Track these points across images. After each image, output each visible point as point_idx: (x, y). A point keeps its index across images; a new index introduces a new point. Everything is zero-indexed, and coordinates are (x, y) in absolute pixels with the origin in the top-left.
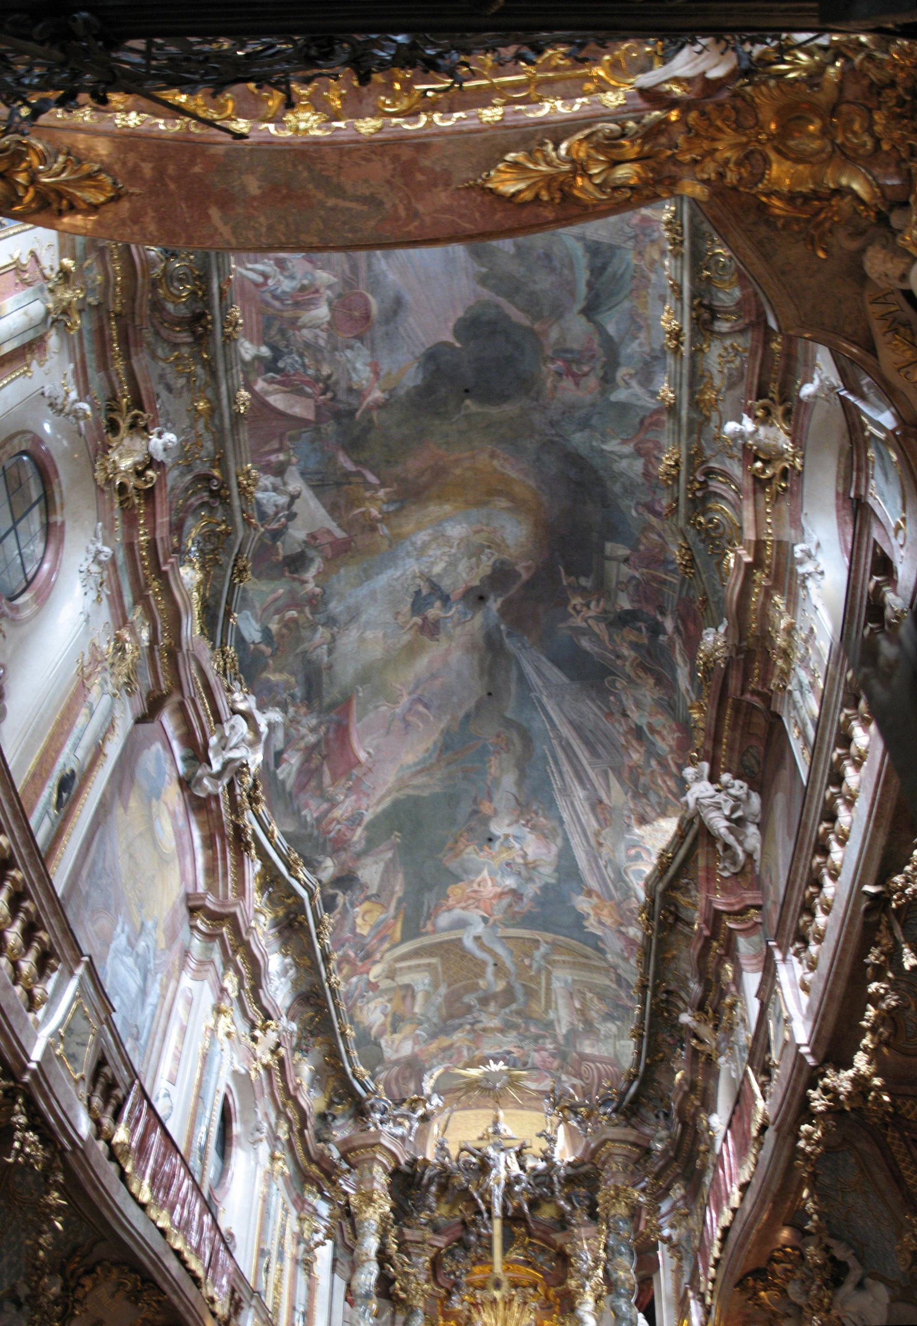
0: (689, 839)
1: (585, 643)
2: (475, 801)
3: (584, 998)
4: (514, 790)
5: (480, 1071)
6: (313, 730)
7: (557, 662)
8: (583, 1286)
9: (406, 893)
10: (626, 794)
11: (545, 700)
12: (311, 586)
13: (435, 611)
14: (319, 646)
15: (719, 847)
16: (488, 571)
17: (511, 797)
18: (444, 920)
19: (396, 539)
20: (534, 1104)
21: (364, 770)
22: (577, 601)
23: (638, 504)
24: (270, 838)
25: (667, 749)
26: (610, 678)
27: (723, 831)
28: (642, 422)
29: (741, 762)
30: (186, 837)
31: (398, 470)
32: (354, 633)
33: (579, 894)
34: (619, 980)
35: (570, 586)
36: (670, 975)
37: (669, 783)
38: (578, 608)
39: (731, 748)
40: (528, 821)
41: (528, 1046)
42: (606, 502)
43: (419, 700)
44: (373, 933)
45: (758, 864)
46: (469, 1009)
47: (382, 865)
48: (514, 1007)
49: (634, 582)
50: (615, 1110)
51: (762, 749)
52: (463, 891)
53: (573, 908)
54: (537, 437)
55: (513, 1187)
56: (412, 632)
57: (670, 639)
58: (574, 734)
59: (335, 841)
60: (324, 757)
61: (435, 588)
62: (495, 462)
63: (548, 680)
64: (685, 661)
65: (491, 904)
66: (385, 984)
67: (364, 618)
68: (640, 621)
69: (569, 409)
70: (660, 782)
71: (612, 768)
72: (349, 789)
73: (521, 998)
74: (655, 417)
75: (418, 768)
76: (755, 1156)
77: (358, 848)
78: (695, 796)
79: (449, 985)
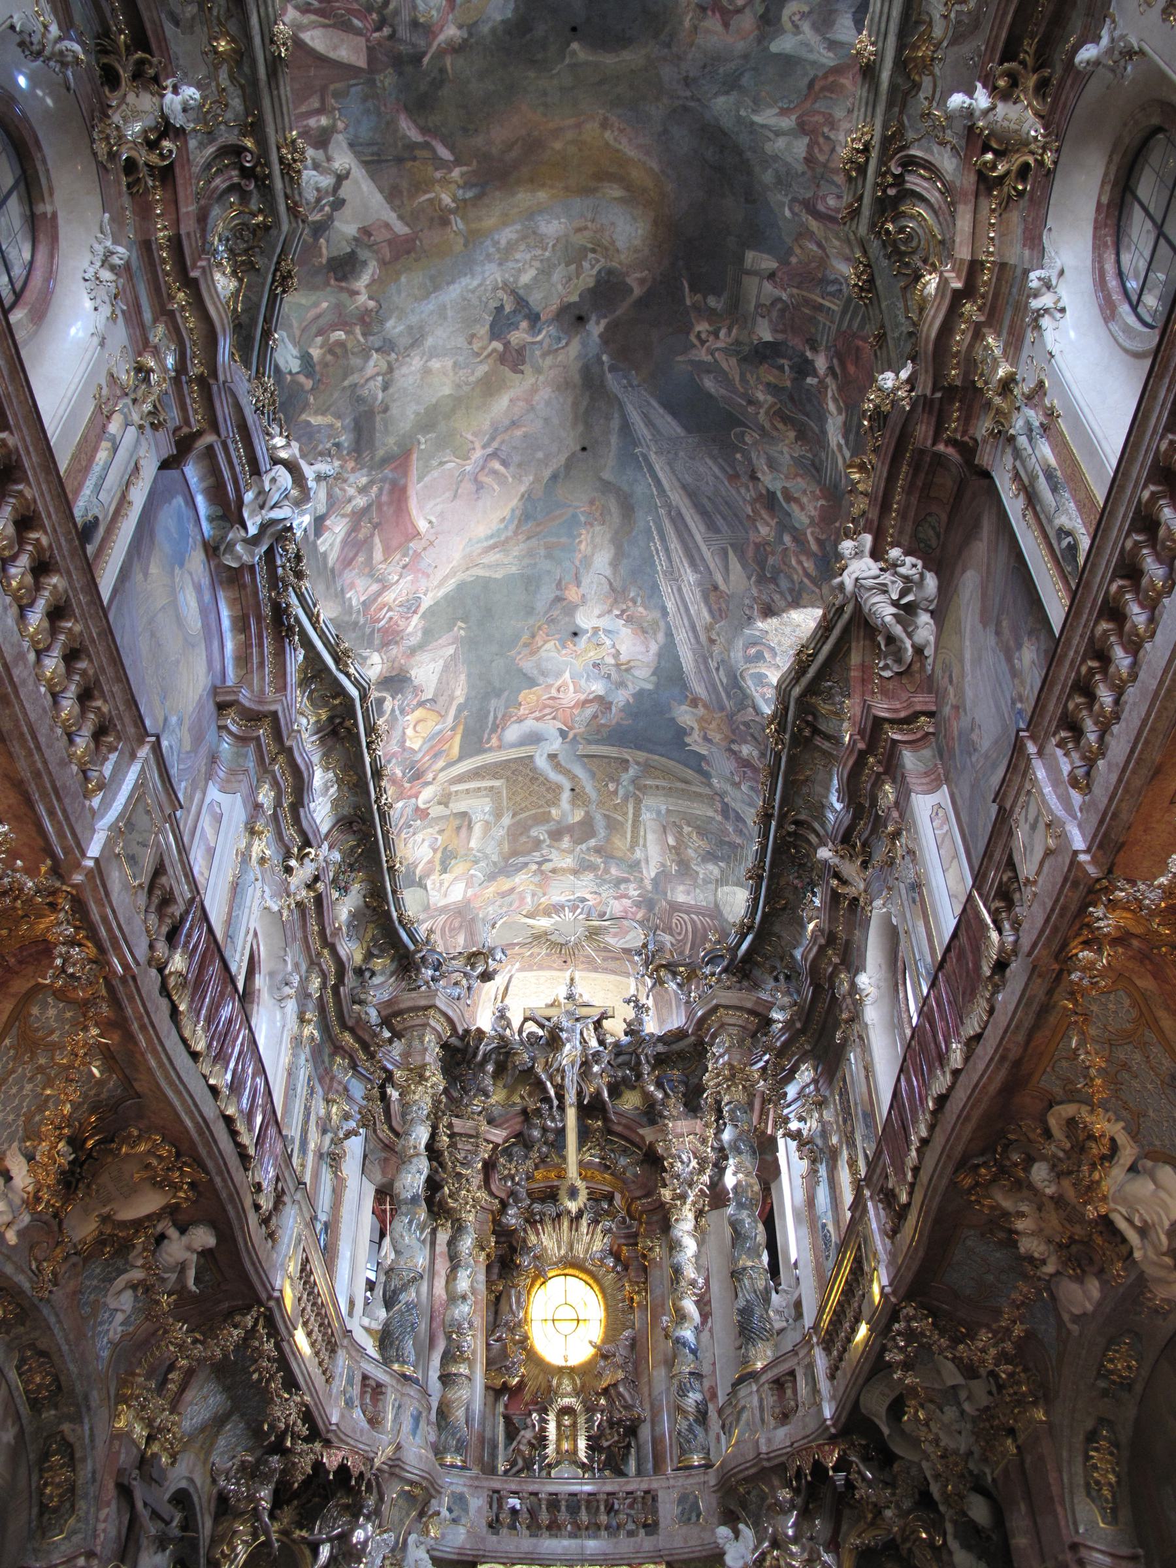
1: (709, 384)
2: (559, 585)
3: (681, 833)
4: (608, 572)
5: (552, 921)
6: (363, 490)
7: (672, 408)
8: (683, 1197)
9: (467, 699)
10: (749, 578)
11: (653, 457)
12: (362, 298)
13: (519, 335)
14: (372, 378)
15: (881, 639)
16: (591, 283)
17: (604, 580)
18: (513, 733)
19: (473, 238)
20: (612, 965)
21: (424, 543)
22: (702, 327)
23: (794, 200)
24: (315, 624)
25: (807, 521)
26: (738, 430)
27: (888, 619)
28: (811, 85)
29: (915, 535)
30: (213, 616)
31: (478, 141)
32: (416, 362)
33: (681, 703)
34: (726, 811)
35: (695, 306)
36: (800, 802)
38: (703, 336)
39: (903, 515)
40: (623, 612)
41: (607, 892)
42: (751, 196)
43: (494, 455)
44: (426, 747)
45: (930, 661)
46: (537, 844)
47: (441, 662)
48: (592, 842)
49: (779, 306)
50: (725, 970)
51: (944, 517)
52: (539, 698)
53: (673, 720)
54: (665, 100)
55: (591, 1067)
56: (490, 361)
57: (821, 382)
58: (687, 501)
59: (385, 631)
60: (375, 527)
61: (521, 303)
62: (607, 134)
63: (658, 432)
64: (840, 412)
65: (572, 714)
66: (436, 811)
67: (429, 342)
68: (783, 357)
69: (713, 61)
70: (794, 562)
71: (732, 545)
72: (404, 567)
73: (602, 832)
75: (491, 542)
76: (988, 1000)
77: (414, 641)
78: (854, 576)
79: (514, 815)
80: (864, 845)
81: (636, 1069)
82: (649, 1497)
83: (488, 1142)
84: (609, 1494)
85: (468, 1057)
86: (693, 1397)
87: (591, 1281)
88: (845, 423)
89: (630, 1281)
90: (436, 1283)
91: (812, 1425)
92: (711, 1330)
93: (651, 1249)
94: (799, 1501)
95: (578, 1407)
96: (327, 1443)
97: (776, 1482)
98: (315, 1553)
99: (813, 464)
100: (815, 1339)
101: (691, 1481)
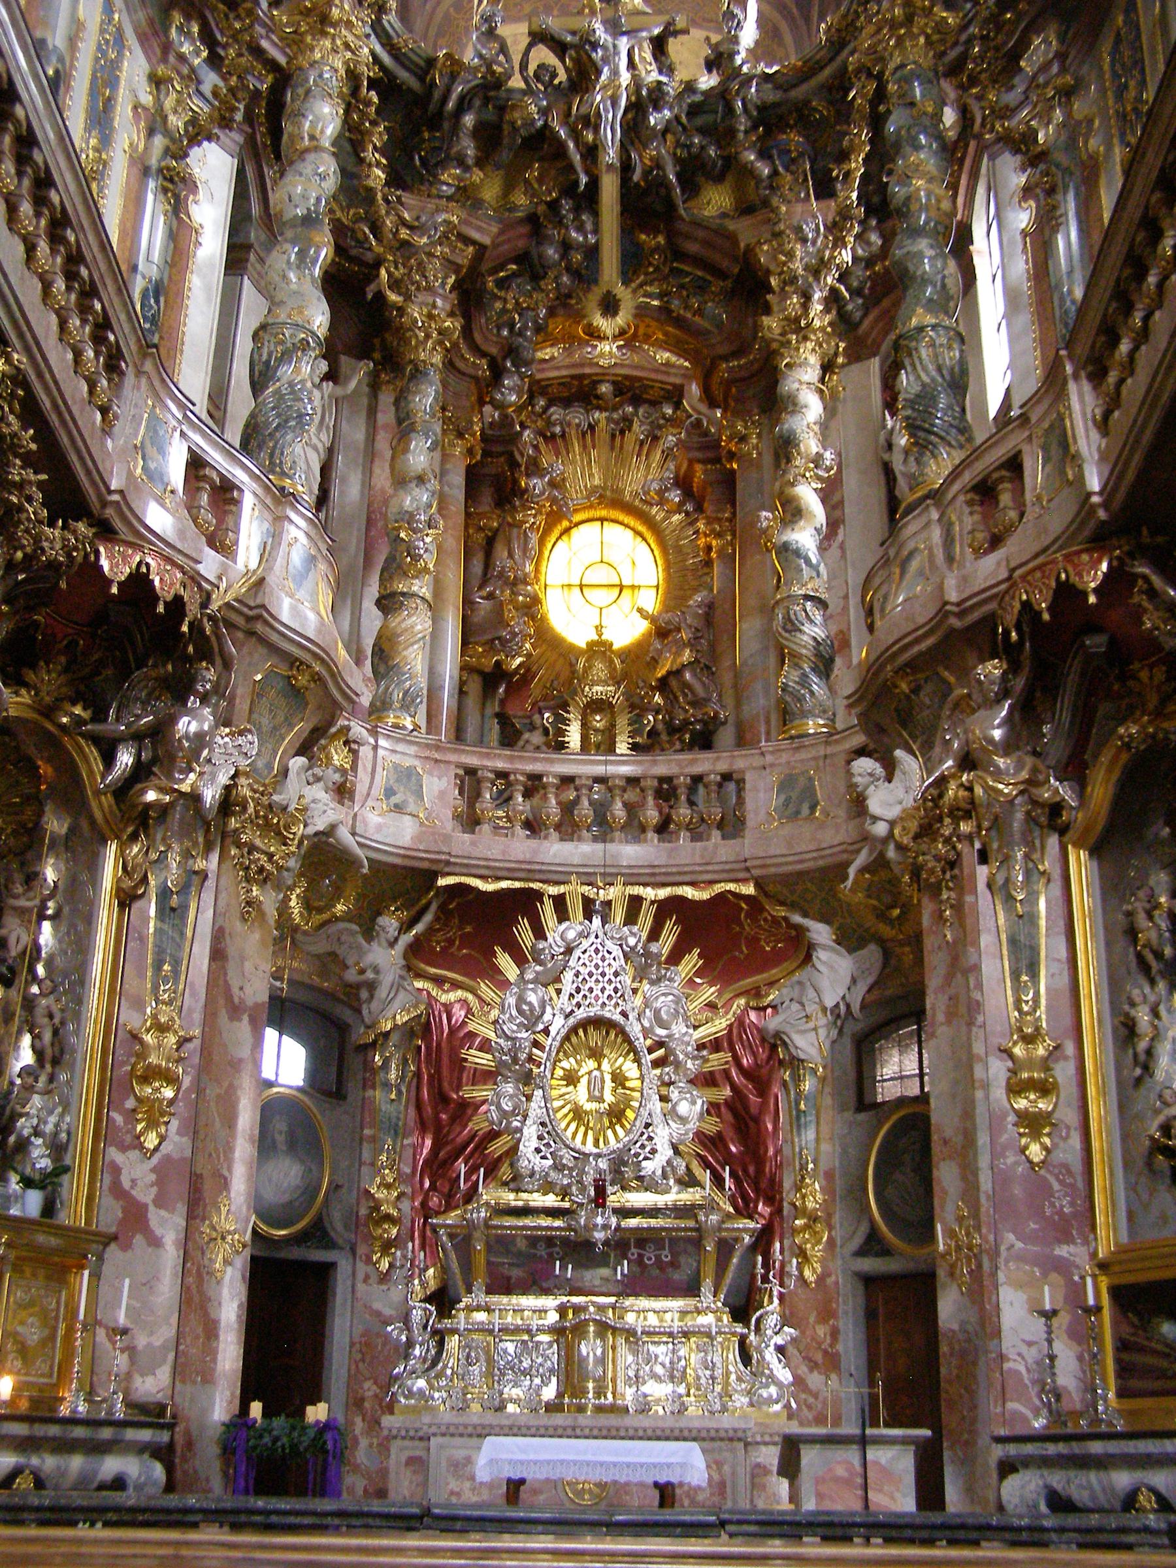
81: (724, 135)
82: (731, 787)
83: (467, 240)
84: (662, 780)
85: (432, 108)
86: (814, 629)
87: (641, 528)
89: (707, 518)
90: (377, 471)
91: (1058, 521)
92: (842, 547)
93: (743, 439)
94: (1019, 683)
95: (618, 699)
96: (106, 531)
97: (971, 658)
98: (109, 759)
100: (1069, 369)
101: (803, 755)
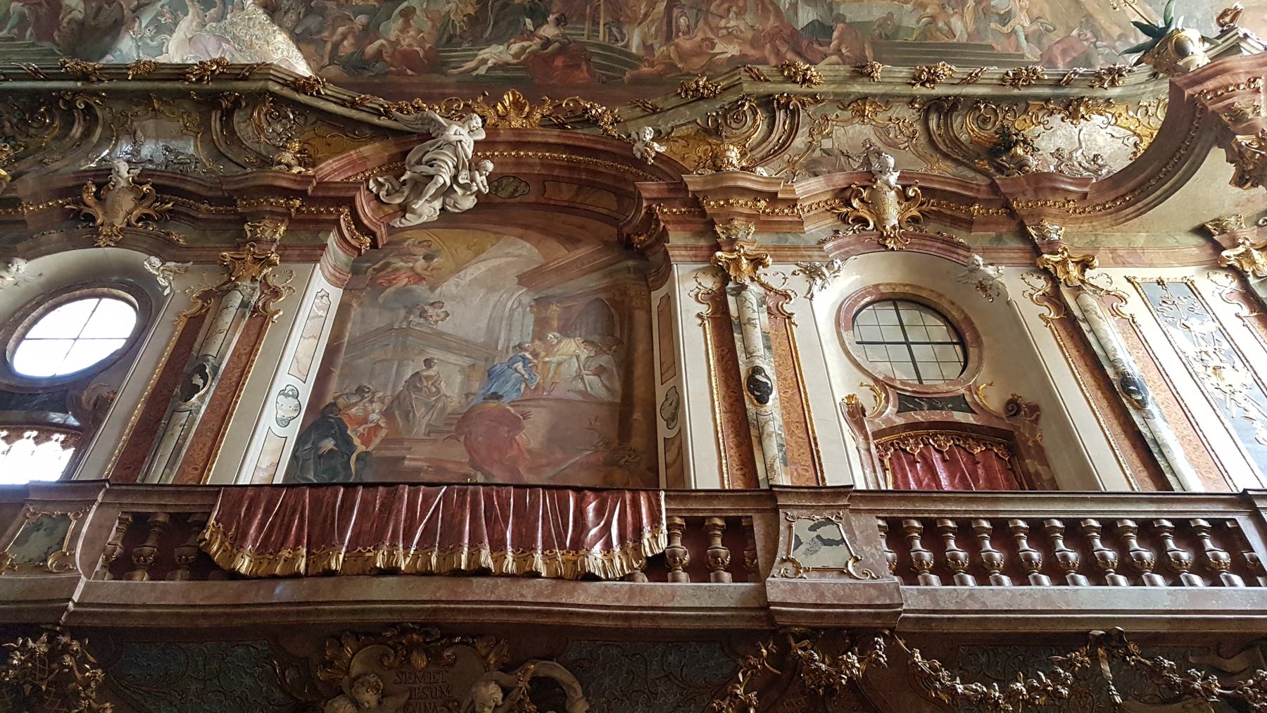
0: (353, 113)
37: (345, 43)
64: (516, 56)
70: (341, 29)
74: (771, 8)
80: (169, 211)
88: (507, 64)
99: (451, 37)
